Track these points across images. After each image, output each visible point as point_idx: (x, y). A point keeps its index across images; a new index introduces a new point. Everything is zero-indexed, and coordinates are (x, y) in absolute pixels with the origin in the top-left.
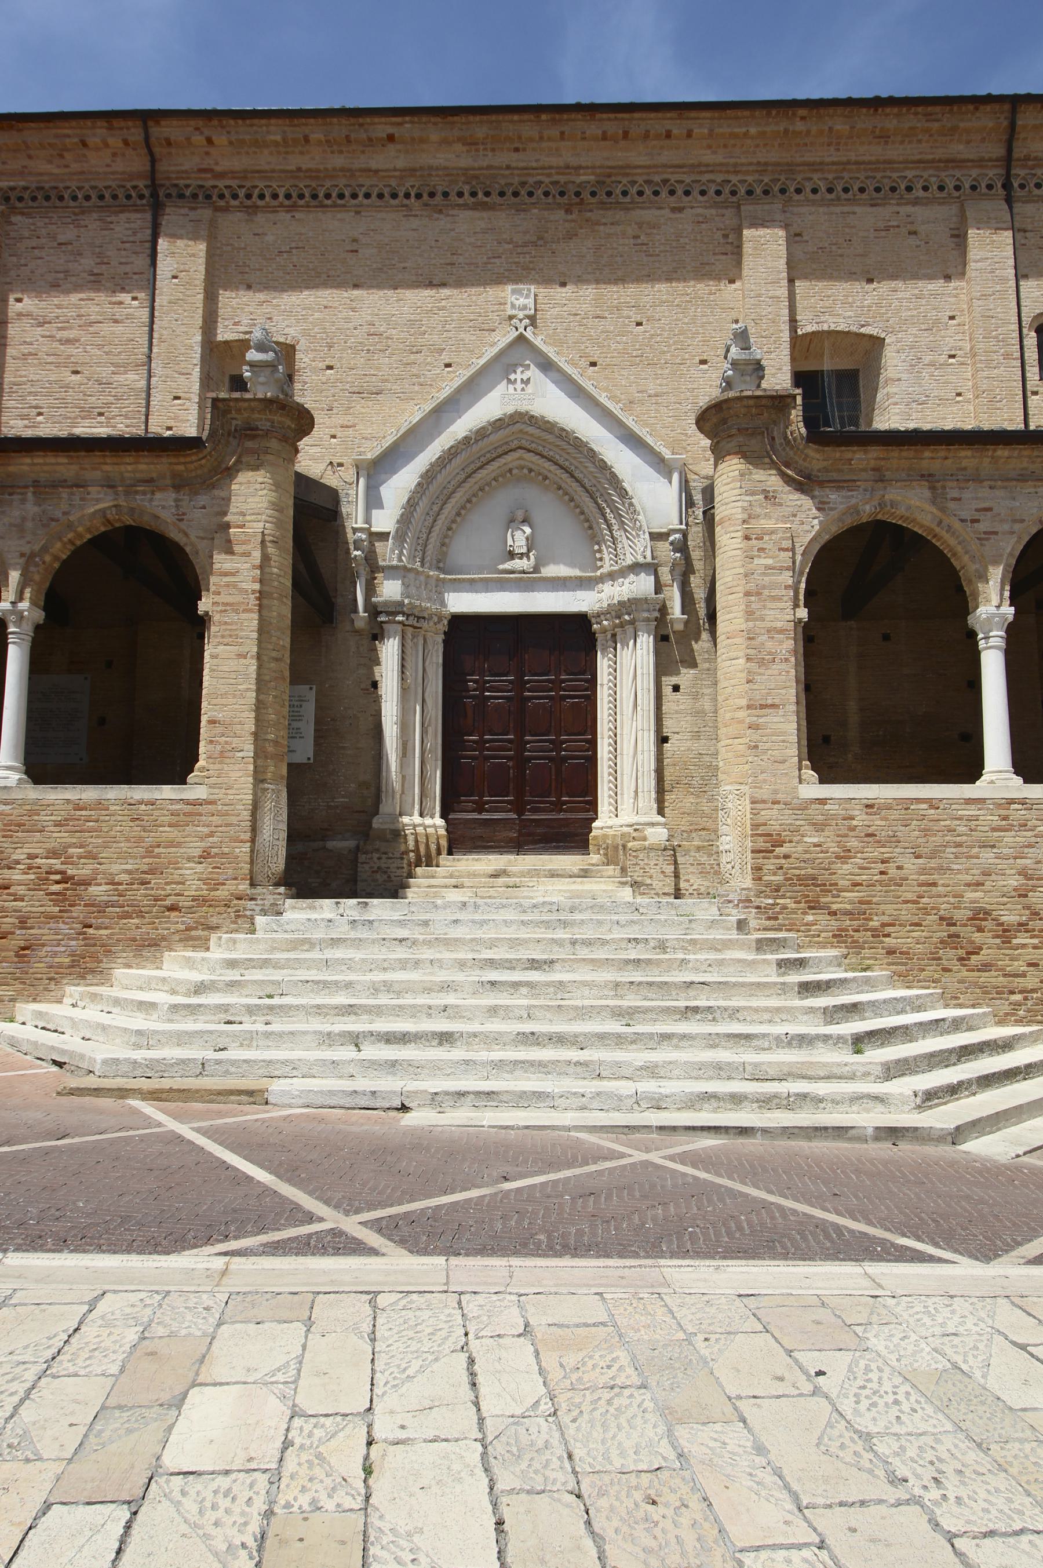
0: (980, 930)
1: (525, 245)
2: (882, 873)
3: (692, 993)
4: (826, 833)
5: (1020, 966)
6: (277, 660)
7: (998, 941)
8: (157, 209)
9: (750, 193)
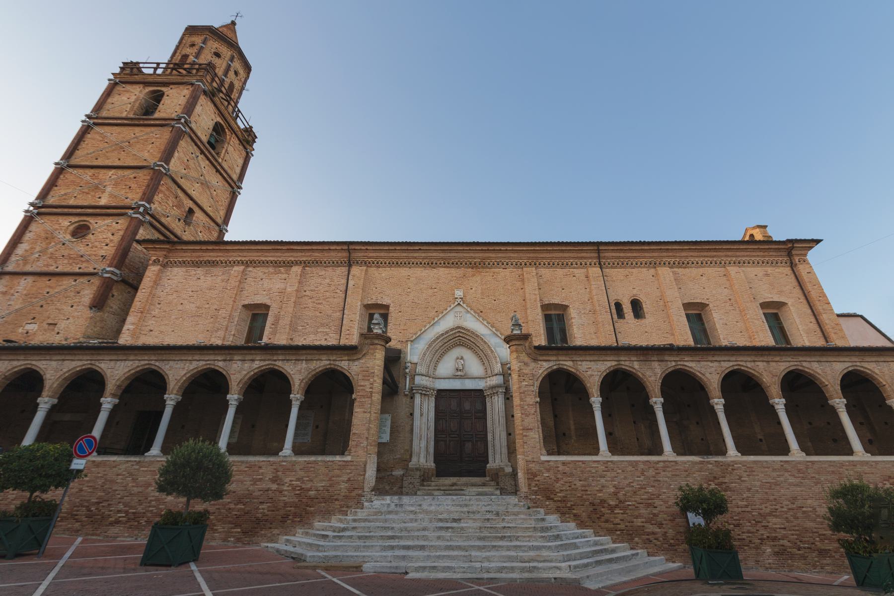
0: (603, 507)
2: (569, 487)
3: (505, 531)
5: (617, 521)
6: (376, 413)
7: (610, 511)
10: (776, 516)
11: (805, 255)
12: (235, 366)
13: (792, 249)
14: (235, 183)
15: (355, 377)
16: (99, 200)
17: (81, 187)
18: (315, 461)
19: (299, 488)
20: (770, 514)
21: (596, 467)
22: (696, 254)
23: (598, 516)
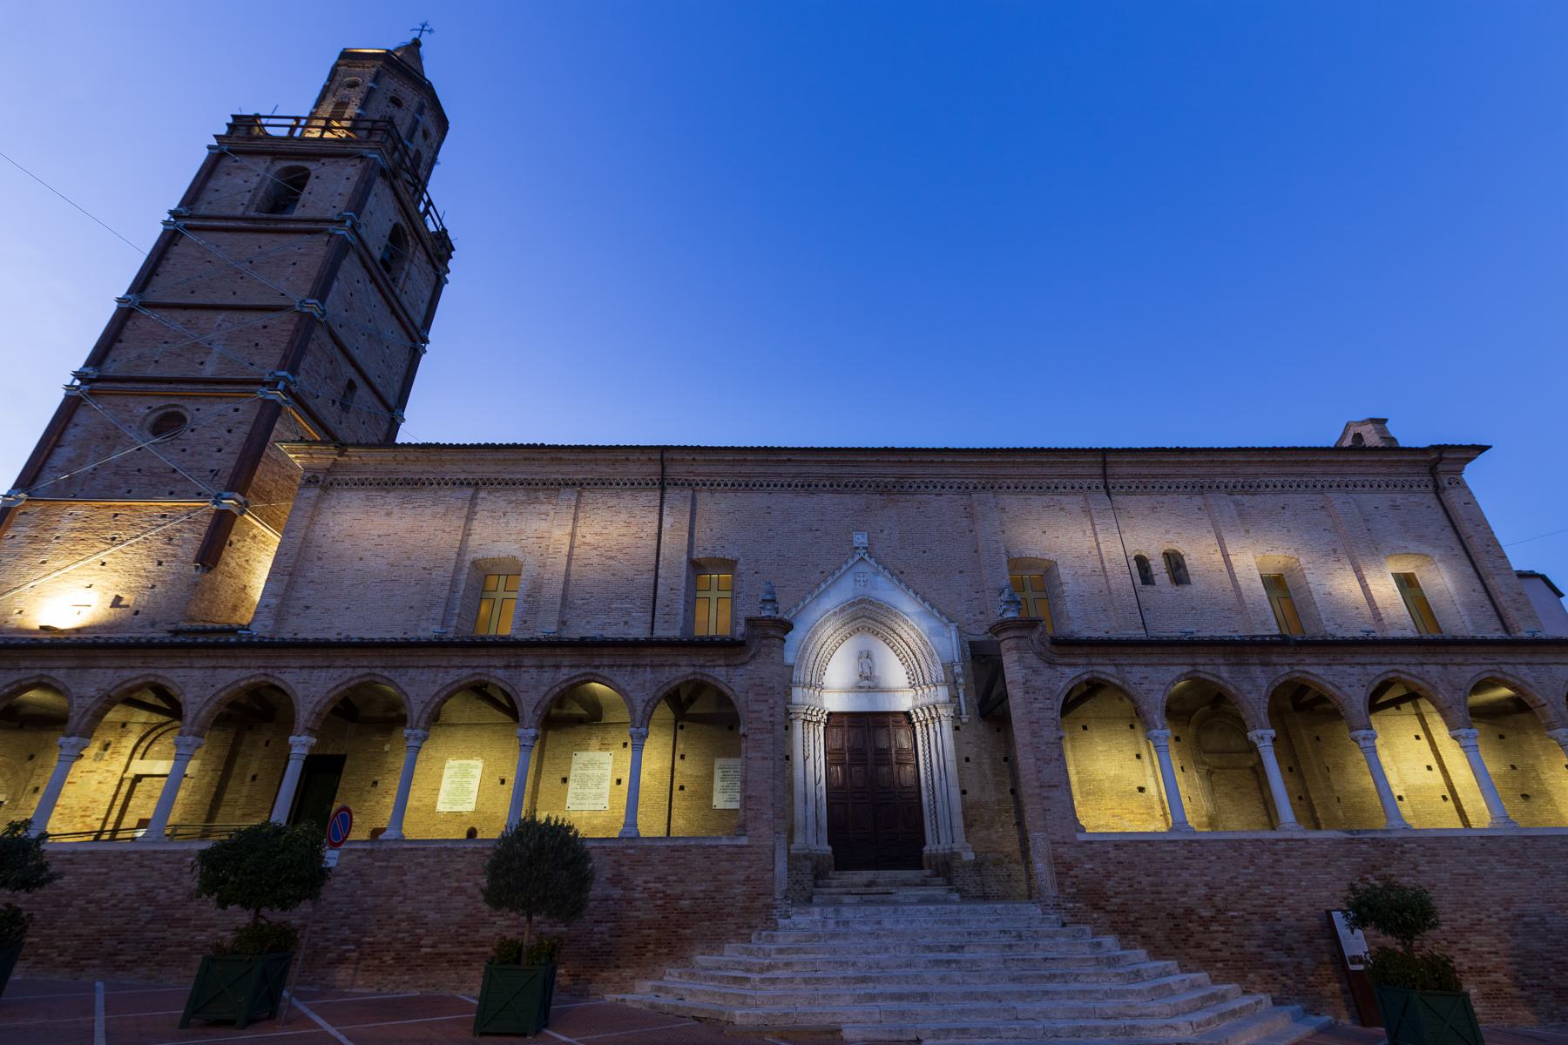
1: (861, 511)
2: (1130, 886)
8: (663, 490)
9: (975, 488)
10: (1481, 933)
11: (1460, 472)
12: (526, 676)
13: (1438, 463)
14: (418, 332)
15: (742, 696)
16: (202, 367)
17: (166, 343)
18: (685, 846)
19: (661, 895)
20: (1470, 929)
21: (1171, 852)
22: (1273, 470)
23: (1183, 937)
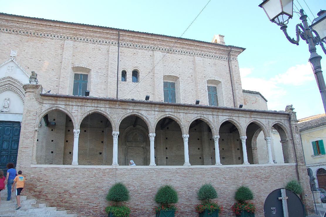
2: (46, 183)
4: (35, 175)
21: (66, 172)
